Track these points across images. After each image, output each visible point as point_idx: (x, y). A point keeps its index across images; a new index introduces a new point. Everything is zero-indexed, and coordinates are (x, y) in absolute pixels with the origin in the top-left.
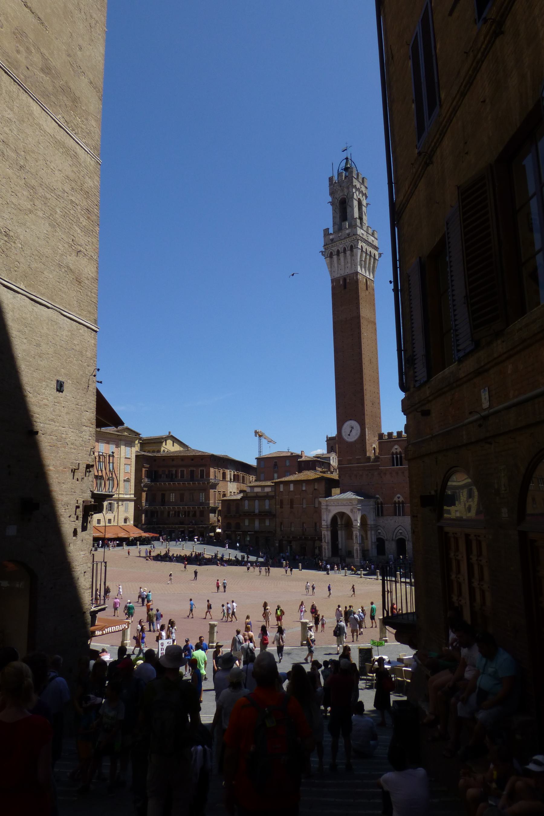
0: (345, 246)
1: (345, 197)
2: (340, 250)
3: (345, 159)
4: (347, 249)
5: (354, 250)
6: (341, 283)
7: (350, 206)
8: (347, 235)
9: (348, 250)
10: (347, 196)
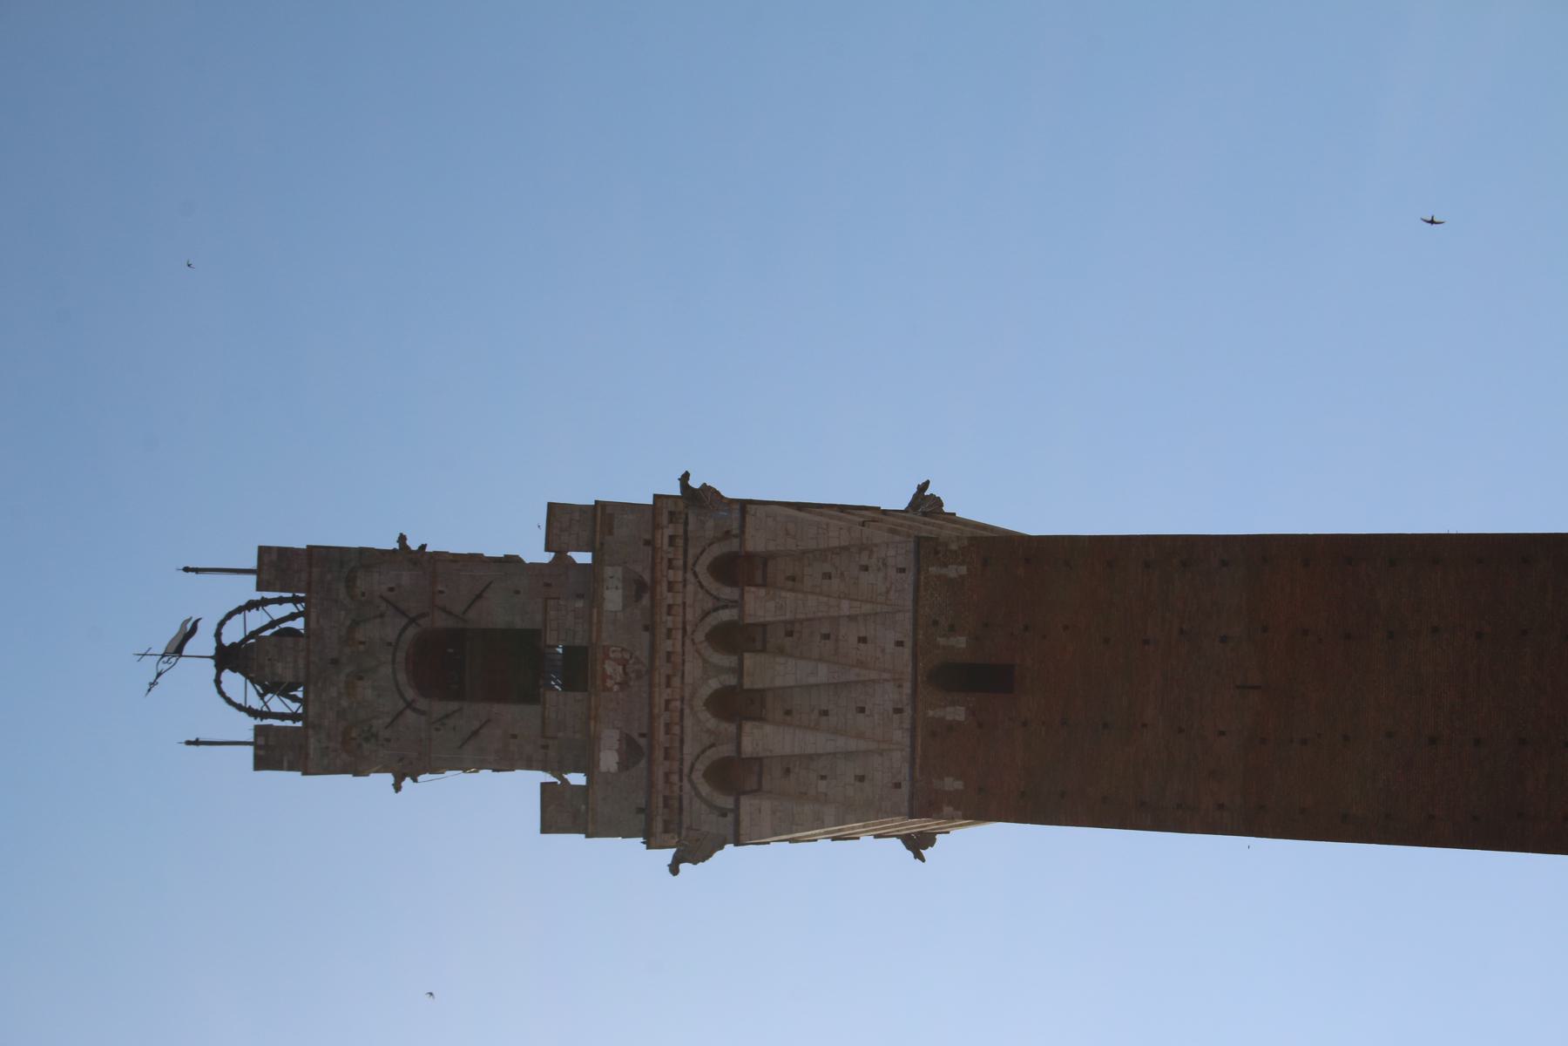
0: (700, 636)
1: (411, 632)
2: (714, 684)
3: (220, 668)
4: (726, 615)
5: (750, 546)
6: (957, 713)
7: (479, 596)
8: (638, 597)
9: (739, 604)
10: (412, 621)
